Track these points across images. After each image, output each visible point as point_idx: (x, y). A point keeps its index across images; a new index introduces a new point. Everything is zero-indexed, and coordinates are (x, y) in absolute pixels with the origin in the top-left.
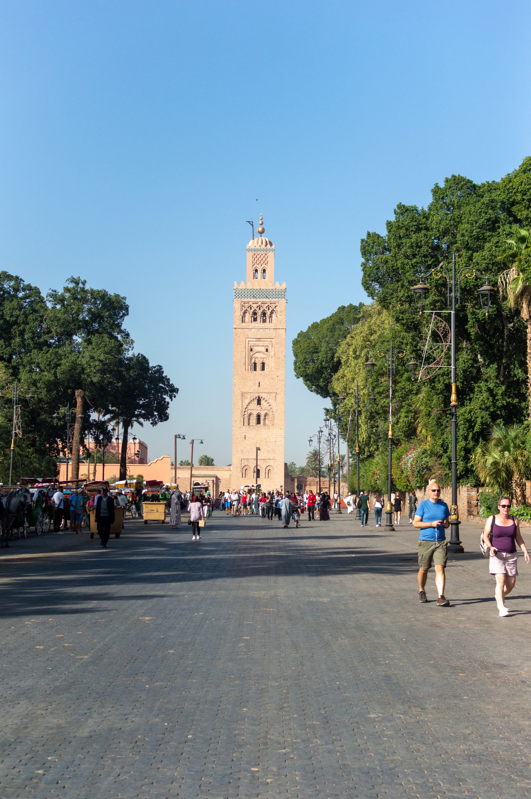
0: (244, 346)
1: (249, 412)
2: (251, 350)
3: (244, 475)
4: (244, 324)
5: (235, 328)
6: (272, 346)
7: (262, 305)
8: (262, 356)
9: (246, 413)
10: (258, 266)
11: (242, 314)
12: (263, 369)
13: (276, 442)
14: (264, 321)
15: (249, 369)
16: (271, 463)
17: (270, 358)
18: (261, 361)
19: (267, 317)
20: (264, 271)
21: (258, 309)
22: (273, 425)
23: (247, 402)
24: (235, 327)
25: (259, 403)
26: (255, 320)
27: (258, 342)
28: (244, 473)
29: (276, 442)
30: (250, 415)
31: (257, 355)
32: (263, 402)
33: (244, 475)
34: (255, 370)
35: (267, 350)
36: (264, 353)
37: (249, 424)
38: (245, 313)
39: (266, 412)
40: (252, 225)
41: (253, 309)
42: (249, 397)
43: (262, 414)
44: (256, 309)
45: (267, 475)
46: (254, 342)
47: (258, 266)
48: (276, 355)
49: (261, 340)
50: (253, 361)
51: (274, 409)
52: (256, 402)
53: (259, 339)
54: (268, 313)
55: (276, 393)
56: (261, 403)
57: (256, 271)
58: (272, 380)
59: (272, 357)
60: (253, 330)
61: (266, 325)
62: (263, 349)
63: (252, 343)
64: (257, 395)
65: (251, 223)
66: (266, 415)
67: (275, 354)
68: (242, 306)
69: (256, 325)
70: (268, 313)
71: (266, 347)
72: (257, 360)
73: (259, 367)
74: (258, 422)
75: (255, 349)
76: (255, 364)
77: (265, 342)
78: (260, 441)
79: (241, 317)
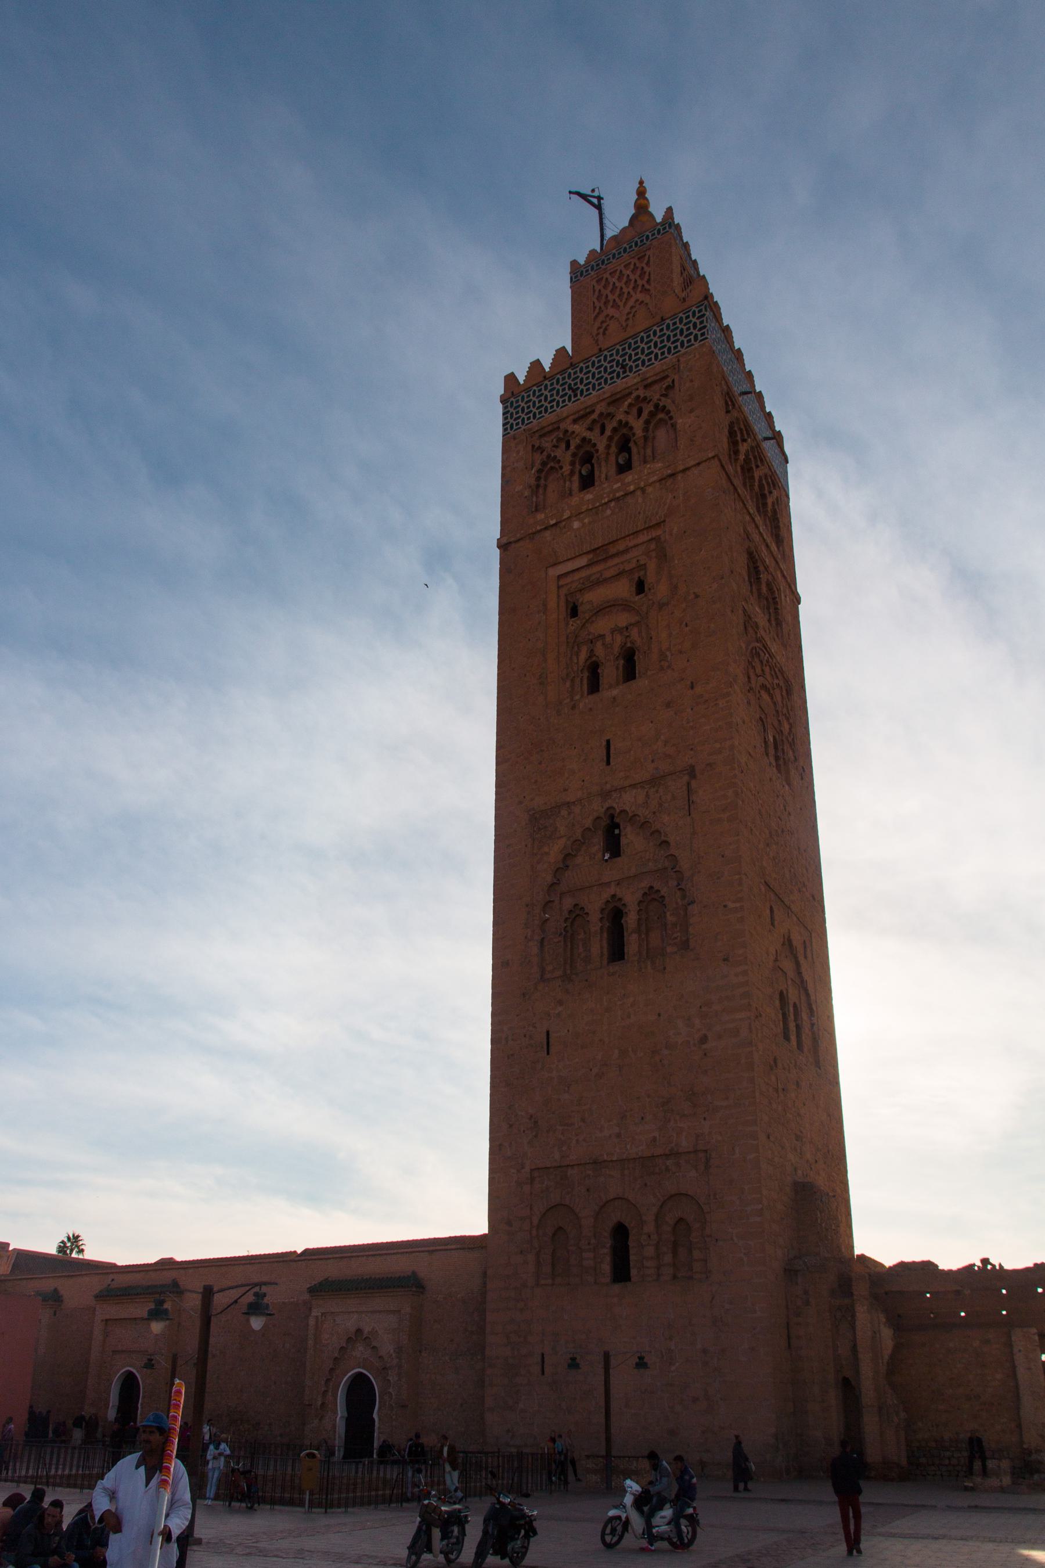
1: (568, 903)
2: (574, 612)
4: (540, 516)
7: (612, 409)
8: (623, 619)
11: (533, 482)
12: (630, 673)
13: (704, 1039)
14: (624, 468)
18: (619, 639)
19: (634, 450)
21: (594, 436)
22: (685, 945)
23: (555, 850)
25: (614, 846)
26: (588, 482)
27: (595, 569)
29: (704, 1039)
36: (625, 606)
39: (645, 884)
43: (631, 898)
44: (587, 434)
46: (584, 573)
50: (583, 655)
52: (597, 843)
53: (600, 554)
55: (691, 772)
56: (624, 841)
59: (661, 606)
62: (622, 589)
64: (598, 807)
66: (651, 896)
69: (589, 496)
70: (638, 425)
71: (636, 576)
73: (610, 672)
77: (628, 556)
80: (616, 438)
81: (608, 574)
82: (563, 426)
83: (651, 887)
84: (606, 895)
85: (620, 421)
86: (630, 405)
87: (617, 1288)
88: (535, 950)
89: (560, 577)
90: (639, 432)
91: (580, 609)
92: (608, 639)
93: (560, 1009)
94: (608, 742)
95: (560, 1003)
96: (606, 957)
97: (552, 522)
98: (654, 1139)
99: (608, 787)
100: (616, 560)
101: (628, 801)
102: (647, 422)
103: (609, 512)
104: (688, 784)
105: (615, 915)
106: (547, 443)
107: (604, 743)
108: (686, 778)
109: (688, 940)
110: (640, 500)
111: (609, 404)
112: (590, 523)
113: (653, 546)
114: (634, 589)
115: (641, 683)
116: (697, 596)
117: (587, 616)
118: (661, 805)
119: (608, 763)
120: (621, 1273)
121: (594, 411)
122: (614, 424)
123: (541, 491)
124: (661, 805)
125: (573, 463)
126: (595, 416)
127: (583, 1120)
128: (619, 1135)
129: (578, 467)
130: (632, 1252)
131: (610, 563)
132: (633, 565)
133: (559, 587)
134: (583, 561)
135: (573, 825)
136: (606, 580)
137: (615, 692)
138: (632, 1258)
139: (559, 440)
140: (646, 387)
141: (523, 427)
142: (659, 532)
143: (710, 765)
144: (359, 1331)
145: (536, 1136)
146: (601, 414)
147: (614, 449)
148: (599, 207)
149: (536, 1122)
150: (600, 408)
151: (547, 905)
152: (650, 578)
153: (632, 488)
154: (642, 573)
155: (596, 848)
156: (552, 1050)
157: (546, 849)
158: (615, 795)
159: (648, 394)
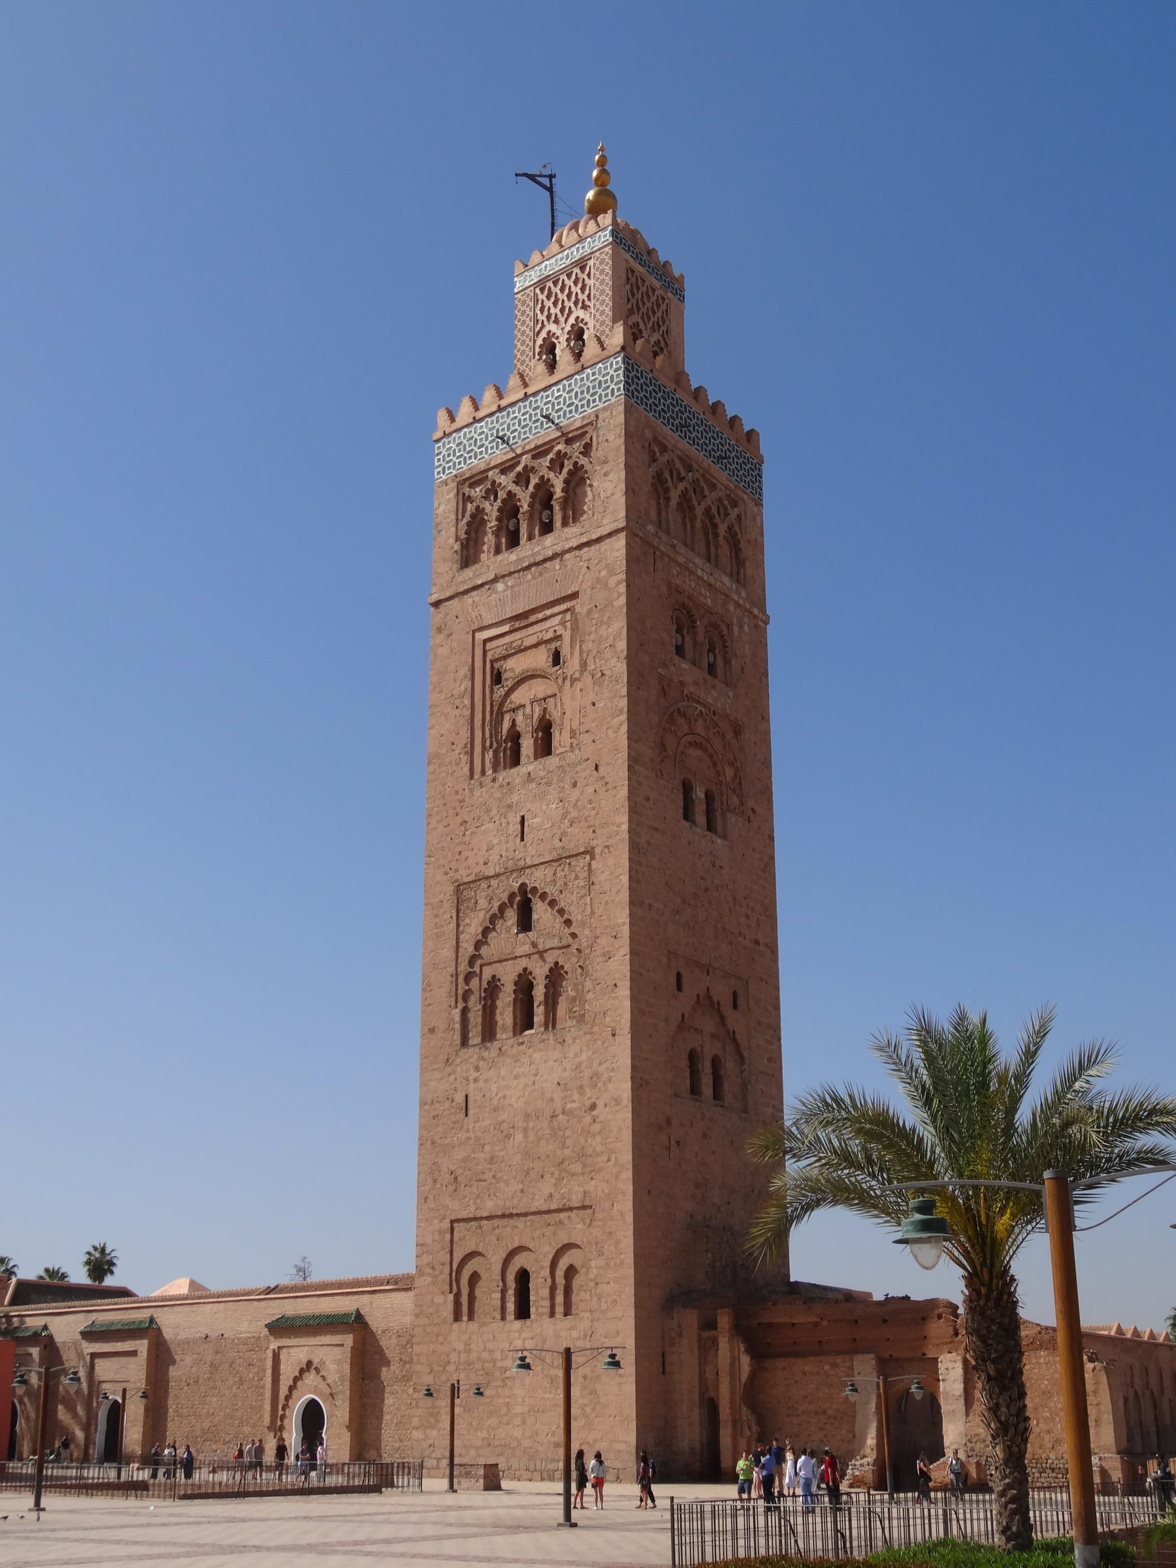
0: (464, 670)
1: (487, 973)
2: (497, 678)
3: (465, 1308)
4: (469, 573)
5: (437, 604)
6: (575, 629)
7: (535, 463)
8: (538, 688)
9: (474, 982)
10: (552, 327)
12: (545, 747)
13: (593, 1107)
14: (547, 528)
15: (488, 764)
16: (575, 1228)
17: (568, 682)
20: (578, 334)
24: (434, 598)
25: (525, 924)
27: (518, 635)
28: (464, 1300)
29: (593, 1107)
30: (493, 988)
31: (518, 697)
32: (540, 911)
33: (465, 1308)
34: (515, 761)
35: (556, 658)
37: (489, 1032)
38: (477, 523)
39: (551, 958)
40: (550, 189)
41: (502, 495)
42: (483, 903)
43: (540, 972)
45: (560, 1299)
46: (508, 639)
47: (552, 327)
48: (591, 667)
49: (532, 619)
50: (506, 725)
51: (585, 934)
52: (512, 916)
53: (522, 619)
54: (558, 485)
55: (590, 852)
56: (535, 916)
57: (549, 348)
58: (575, 793)
60: (500, 586)
61: (549, 544)
62: (540, 659)
63: (497, 648)
65: (546, 183)
67: (584, 665)
68: (468, 499)
70: (558, 485)
71: (553, 645)
72: (520, 719)
73: (527, 745)
74: (525, 1021)
75: (515, 666)
76: (515, 737)
78: (527, 1117)
79: (457, 547)
80: (540, 494)
81: (529, 642)
82: (490, 473)
83: (556, 963)
84: (519, 969)
85: (543, 477)
86: (552, 460)
87: (518, 1324)
88: (457, 1018)
89: (485, 641)
90: (558, 493)
91: (504, 676)
92: (528, 710)
93: (476, 1075)
94: (523, 817)
95: (477, 1069)
96: (518, 1027)
97: (479, 582)
98: (551, 1195)
99: (522, 863)
100: (536, 628)
101: (538, 878)
102: (567, 481)
103: (529, 577)
104: (589, 864)
105: (524, 985)
106: (478, 491)
107: (519, 819)
108: (588, 857)
109: (584, 1015)
110: (557, 567)
111: (534, 457)
112: (513, 587)
113: (568, 616)
114: (550, 659)
115: (552, 761)
116: (603, 675)
117: (509, 683)
118: (566, 884)
119: (522, 839)
120: (523, 1312)
121: (518, 463)
122: (537, 480)
123: (472, 543)
124: (566, 884)
125: (499, 519)
126: (519, 468)
127: (494, 1177)
128: (522, 1191)
129: (505, 521)
130: (531, 1293)
131: (531, 630)
132: (550, 635)
133: (485, 652)
134: (506, 628)
135: (492, 898)
136: (526, 649)
137: (530, 768)
138: (532, 1298)
139: (488, 492)
140: (569, 442)
141: (455, 472)
142: (573, 603)
143: (607, 847)
144: (309, 1363)
145: (455, 1190)
146: (526, 467)
147: (537, 506)
148: (550, 189)
149: (456, 1178)
150: (525, 459)
151: (468, 978)
152: (565, 651)
153: (550, 553)
154: (559, 643)
155: (509, 923)
156: (471, 1112)
157: (467, 921)
158: (527, 871)
159: (569, 450)
